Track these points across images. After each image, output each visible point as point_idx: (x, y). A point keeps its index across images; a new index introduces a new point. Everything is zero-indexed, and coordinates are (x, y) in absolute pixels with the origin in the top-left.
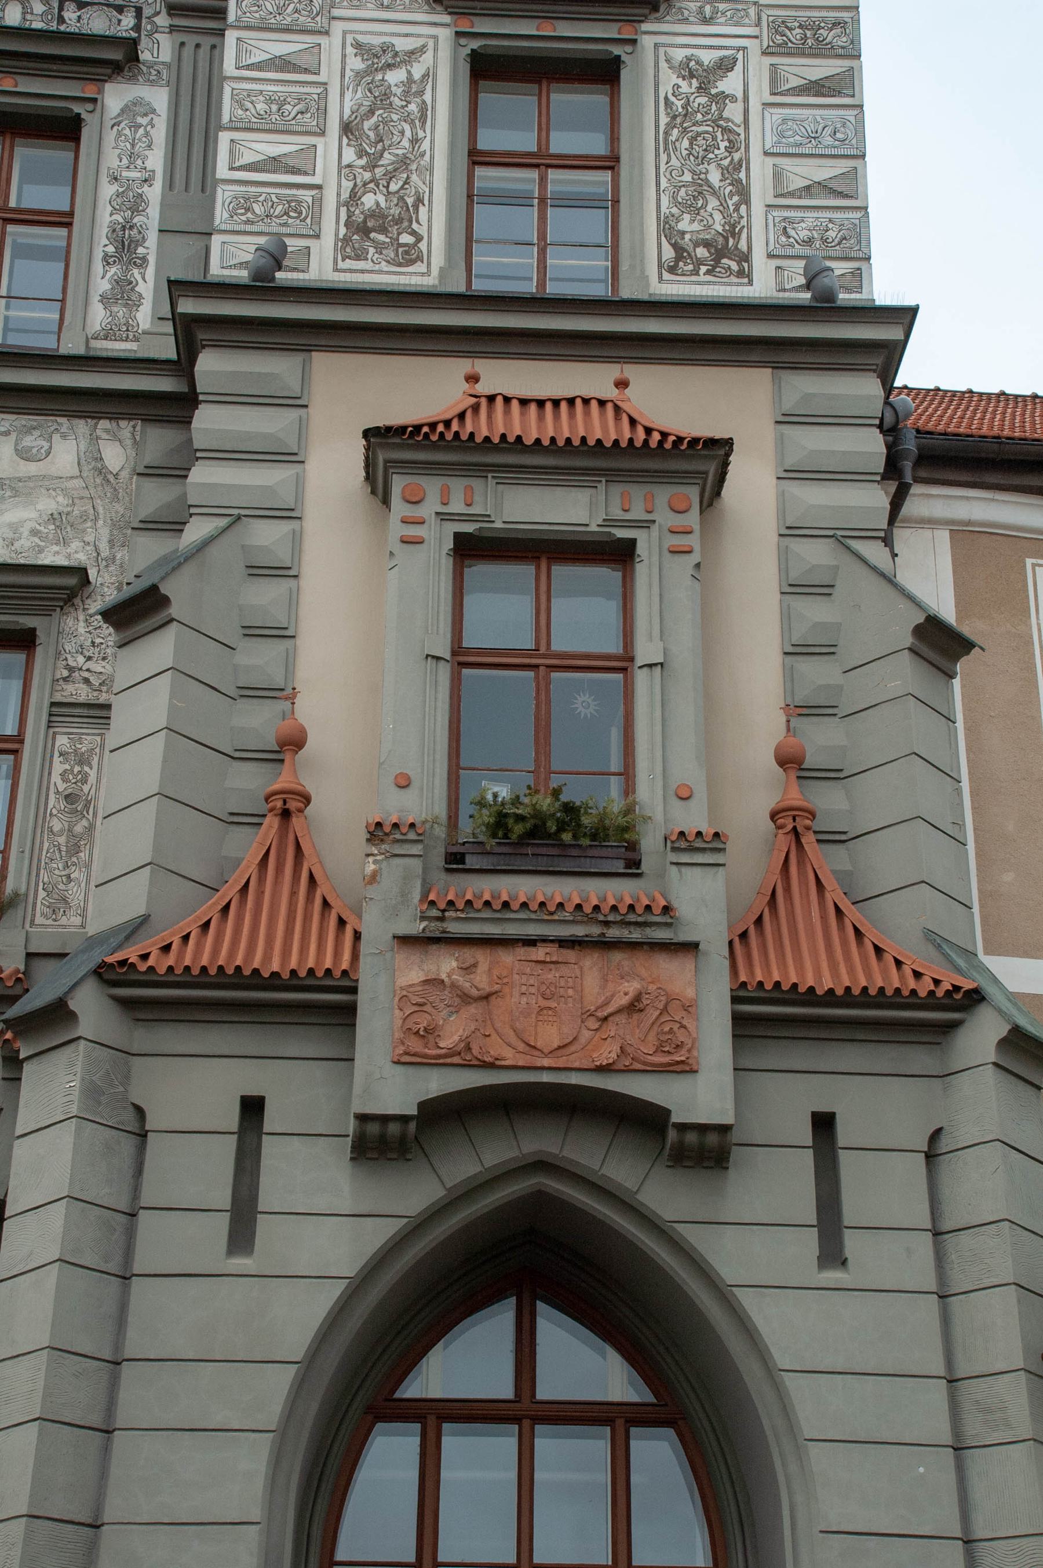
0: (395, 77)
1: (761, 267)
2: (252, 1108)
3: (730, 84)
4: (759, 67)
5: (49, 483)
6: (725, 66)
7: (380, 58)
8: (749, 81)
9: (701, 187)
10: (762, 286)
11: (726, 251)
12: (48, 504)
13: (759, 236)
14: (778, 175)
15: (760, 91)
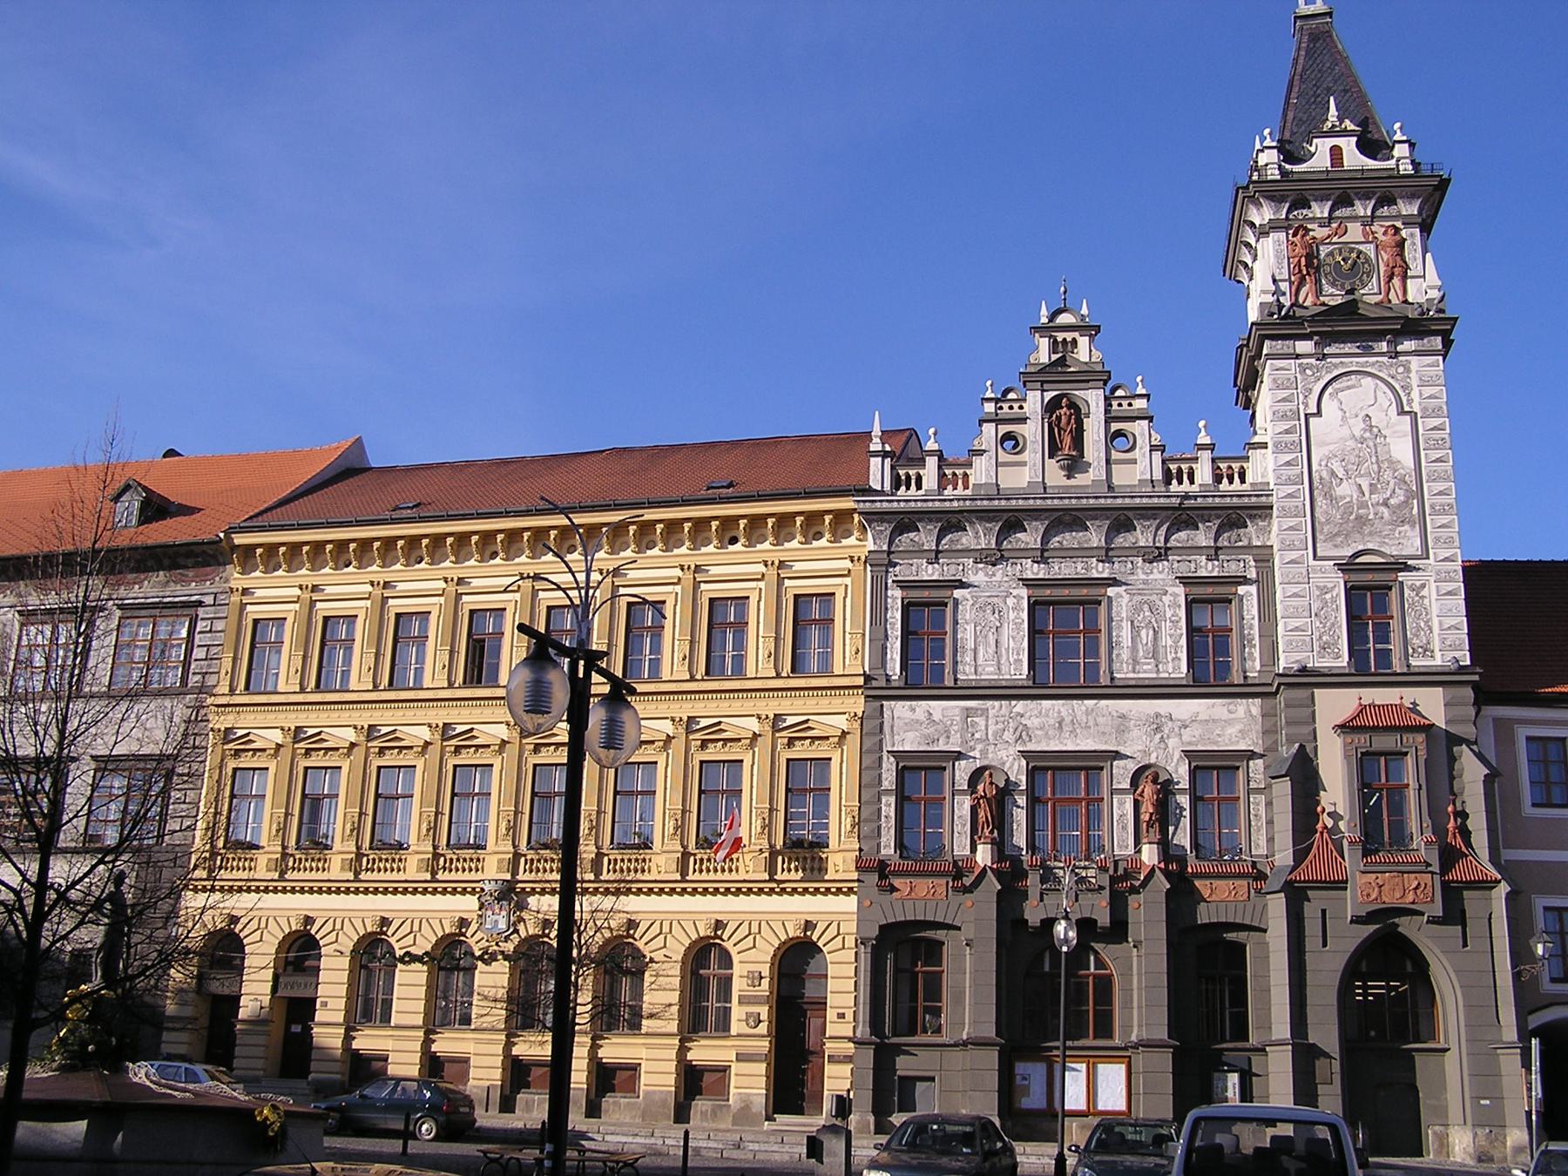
0: (1328, 596)
1: (1438, 654)
2: (1324, 911)
3: (1424, 592)
4: (1433, 585)
5: (1238, 720)
6: (1423, 586)
7: (1324, 590)
8: (1431, 591)
9: (1419, 628)
10: (1438, 662)
11: (1427, 650)
12: (1239, 727)
13: (1436, 645)
14: (1441, 623)
15: (1434, 596)
